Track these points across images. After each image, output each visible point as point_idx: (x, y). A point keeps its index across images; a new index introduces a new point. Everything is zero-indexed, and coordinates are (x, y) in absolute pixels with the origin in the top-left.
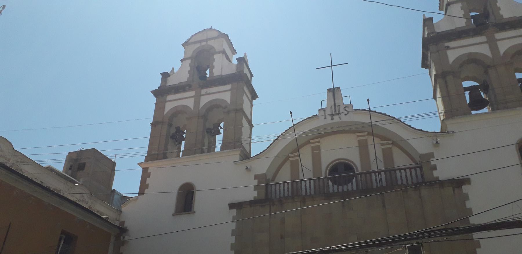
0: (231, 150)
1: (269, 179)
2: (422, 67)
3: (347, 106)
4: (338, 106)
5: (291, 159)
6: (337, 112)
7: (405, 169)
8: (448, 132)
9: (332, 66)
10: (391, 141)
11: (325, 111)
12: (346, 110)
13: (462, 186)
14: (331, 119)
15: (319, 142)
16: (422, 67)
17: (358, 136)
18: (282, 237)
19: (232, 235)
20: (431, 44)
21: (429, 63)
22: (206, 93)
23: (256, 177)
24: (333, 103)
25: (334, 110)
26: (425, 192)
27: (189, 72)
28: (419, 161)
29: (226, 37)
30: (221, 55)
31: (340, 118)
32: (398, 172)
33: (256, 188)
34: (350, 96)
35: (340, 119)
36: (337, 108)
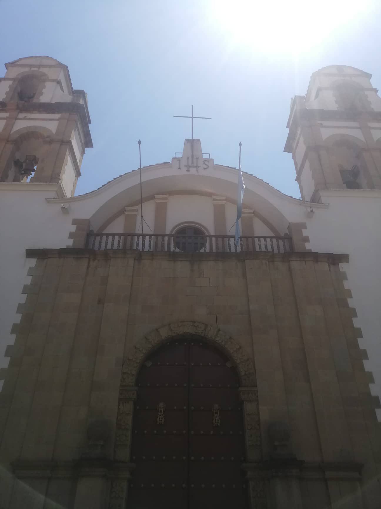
0: (45, 184)
2: (284, 151)
3: (206, 160)
4: (197, 158)
5: (127, 213)
6: (195, 165)
7: (271, 238)
8: (323, 203)
9: (192, 117)
10: (253, 210)
12: (205, 164)
13: (339, 264)
14: (187, 171)
15: (166, 199)
17: (214, 200)
18: (100, 302)
19: (24, 292)
22: (25, 117)
23: (75, 222)
26: (296, 264)
27: (7, 93)
28: (286, 234)
29: (65, 68)
30: (55, 84)
31: (197, 171)
32: (262, 240)
33: (71, 235)
34: (210, 154)
35: (198, 172)
36: (195, 160)
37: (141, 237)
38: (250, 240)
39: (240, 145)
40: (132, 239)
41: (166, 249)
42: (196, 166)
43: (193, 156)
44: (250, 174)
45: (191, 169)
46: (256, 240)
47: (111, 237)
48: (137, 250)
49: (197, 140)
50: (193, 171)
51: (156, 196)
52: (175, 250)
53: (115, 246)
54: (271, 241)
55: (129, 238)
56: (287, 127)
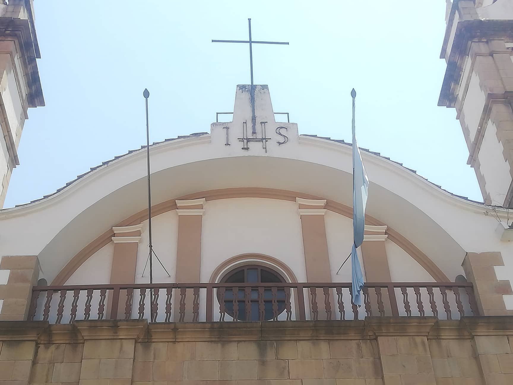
1: (43, 280)
2: (441, 103)
4: (262, 123)
5: (115, 240)
6: (259, 136)
7: (429, 286)
9: (251, 42)
11: (227, 128)
12: (280, 134)
14: (242, 148)
16: (440, 104)
17: (301, 207)
20: (476, 40)
21: (460, 92)
24: (249, 116)
25: (250, 131)
28: (460, 277)
32: (410, 291)
34: (288, 114)
36: (258, 127)
37: (148, 290)
38: (385, 291)
39: (353, 94)
40: (130, 296)
41: (203, 317)
42: (262, 139)
43: (254, 119)
44: (375, 153)
45: (251, 145)
46: (398, 291)
47: (83, 294)
48: (141, 320)
49: (261, 85)
50: (256, 149)
51: (179, 203)
52: (222, 317)
53: (94, 315)
54: (431, 293)
55: (123, 293)
56: (442, 56)
